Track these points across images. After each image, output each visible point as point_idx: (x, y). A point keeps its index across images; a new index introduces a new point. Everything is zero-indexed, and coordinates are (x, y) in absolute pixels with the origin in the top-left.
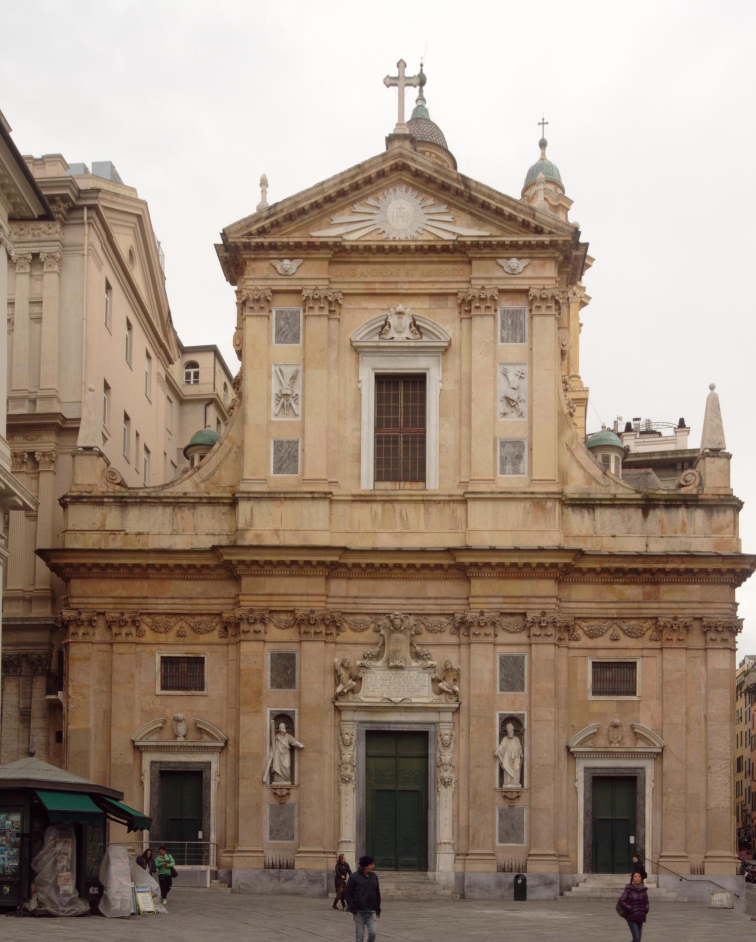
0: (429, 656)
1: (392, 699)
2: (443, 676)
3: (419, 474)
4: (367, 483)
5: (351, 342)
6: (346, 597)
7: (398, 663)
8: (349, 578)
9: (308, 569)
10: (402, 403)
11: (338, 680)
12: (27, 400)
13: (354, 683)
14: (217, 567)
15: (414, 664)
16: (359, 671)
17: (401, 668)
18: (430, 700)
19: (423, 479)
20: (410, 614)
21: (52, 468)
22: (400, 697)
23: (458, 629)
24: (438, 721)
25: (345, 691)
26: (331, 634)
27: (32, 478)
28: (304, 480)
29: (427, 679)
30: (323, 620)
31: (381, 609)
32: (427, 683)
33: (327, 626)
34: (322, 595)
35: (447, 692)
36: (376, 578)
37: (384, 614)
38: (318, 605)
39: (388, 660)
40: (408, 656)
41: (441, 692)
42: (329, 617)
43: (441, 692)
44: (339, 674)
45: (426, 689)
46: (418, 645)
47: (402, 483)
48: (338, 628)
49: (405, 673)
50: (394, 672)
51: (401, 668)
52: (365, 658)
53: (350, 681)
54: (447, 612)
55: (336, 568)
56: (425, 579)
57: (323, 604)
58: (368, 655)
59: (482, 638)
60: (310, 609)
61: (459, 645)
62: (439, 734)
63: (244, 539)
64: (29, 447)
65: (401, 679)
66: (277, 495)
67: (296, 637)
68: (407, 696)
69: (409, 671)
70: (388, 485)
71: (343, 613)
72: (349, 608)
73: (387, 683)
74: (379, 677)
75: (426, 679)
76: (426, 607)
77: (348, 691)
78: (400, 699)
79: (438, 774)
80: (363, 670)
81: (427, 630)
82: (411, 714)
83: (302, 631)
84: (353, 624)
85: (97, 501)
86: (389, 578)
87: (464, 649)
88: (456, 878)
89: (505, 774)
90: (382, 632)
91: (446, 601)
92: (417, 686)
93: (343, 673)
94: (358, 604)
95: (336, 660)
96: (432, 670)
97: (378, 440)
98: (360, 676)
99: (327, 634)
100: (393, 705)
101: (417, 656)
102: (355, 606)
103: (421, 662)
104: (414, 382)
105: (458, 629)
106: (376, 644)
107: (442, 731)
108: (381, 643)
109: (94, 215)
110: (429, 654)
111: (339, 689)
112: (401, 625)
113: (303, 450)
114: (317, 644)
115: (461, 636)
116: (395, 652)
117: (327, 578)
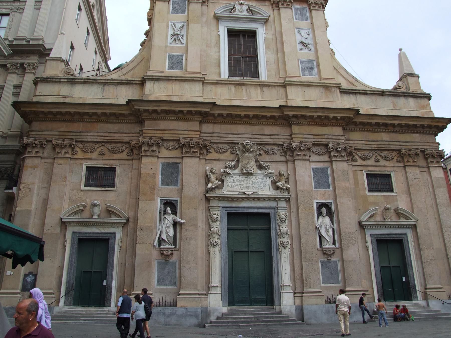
0: (269, 167)
1: (245, 192)
2: (278, 179)
4: (224, 74)
5: (215, 14)
6: (213, 133)
7: (249, 170)
8: (215, 123)
9: (189, 116)
11: (208, 180)
12: (25, 40)
13: (220, 182)
14: (130, 115)
15: (259, 172)
16: (222, 176)
17: (251, 174)
18: (271, 194)
19: (256, 75)
21: (34, 71)
22: (250, 191)
23: (285, 152)
24: (276, 206)
25: (214, 187)
26: (203, 153)
27: (20, 77)
28: (186, 72)
29: (268, 181)
30: (198, 145)
31: (235, 140)
32: (268, 183)
33: (201, 148)
34: (198, 131)
35: (282, 189)
36: (232, 124)
38: (195, 136)
39: (242, 170)
40: (255, 167)
41: (278, 188)
42: (202, 143)
43: (278, 188)
44: (209, 177)
45: (268, 187)
46: (261, 161)
48: (208, 151)
49: (254, 177)
50: (246, 176)
51: (251, 174)
52: (226, 168)
53: (217, 181)
54: (278, 143)
55: (207, 116)
56: (263, 125)
57: (198, 136)
58: (229, 166)
59: (301, 158)
61: (287, 162)
62: (277, 214)
64: (21, 61)
65: (251, 181)
66: (170, 78)
67: (181, 156)
68: (255, 191)
69: (256, 176)
71: (211, 143)
72: (215, 139)
74: (236, 179)
75: (268, 181)
76: (264, 140)
77: (215, 187)
79: (278, 240)
80: (224, 175)
81: (265, 153)
82: (258, 202)
83: (184, 151)
84: (217, 148)
86: (240, 124)
87: (290, 165)
88: (297, 309)
89: (322, 239)
90: (237, 153)
91: (277, 137)
92: (262, 185)
93: (213, 177)
94: (220, 137)
95: (207, 168)
96: (270, 176)
98: (223, 178)
99: (200, 154)
100: (247, 196)
101: (260, 167)
102: (219, 138)
103: (263, 171)
104: (249, 36)
105: (285, 152)
106: (233, 161)
107: (280, 212)
108: (236, 159)
110: (269, 165)
111: (210, 185)
112: (250, 148)
113: (186, 59)
114: (193, 159)
115: (288, 157)
116: (246, 164)
117: (201, 122)
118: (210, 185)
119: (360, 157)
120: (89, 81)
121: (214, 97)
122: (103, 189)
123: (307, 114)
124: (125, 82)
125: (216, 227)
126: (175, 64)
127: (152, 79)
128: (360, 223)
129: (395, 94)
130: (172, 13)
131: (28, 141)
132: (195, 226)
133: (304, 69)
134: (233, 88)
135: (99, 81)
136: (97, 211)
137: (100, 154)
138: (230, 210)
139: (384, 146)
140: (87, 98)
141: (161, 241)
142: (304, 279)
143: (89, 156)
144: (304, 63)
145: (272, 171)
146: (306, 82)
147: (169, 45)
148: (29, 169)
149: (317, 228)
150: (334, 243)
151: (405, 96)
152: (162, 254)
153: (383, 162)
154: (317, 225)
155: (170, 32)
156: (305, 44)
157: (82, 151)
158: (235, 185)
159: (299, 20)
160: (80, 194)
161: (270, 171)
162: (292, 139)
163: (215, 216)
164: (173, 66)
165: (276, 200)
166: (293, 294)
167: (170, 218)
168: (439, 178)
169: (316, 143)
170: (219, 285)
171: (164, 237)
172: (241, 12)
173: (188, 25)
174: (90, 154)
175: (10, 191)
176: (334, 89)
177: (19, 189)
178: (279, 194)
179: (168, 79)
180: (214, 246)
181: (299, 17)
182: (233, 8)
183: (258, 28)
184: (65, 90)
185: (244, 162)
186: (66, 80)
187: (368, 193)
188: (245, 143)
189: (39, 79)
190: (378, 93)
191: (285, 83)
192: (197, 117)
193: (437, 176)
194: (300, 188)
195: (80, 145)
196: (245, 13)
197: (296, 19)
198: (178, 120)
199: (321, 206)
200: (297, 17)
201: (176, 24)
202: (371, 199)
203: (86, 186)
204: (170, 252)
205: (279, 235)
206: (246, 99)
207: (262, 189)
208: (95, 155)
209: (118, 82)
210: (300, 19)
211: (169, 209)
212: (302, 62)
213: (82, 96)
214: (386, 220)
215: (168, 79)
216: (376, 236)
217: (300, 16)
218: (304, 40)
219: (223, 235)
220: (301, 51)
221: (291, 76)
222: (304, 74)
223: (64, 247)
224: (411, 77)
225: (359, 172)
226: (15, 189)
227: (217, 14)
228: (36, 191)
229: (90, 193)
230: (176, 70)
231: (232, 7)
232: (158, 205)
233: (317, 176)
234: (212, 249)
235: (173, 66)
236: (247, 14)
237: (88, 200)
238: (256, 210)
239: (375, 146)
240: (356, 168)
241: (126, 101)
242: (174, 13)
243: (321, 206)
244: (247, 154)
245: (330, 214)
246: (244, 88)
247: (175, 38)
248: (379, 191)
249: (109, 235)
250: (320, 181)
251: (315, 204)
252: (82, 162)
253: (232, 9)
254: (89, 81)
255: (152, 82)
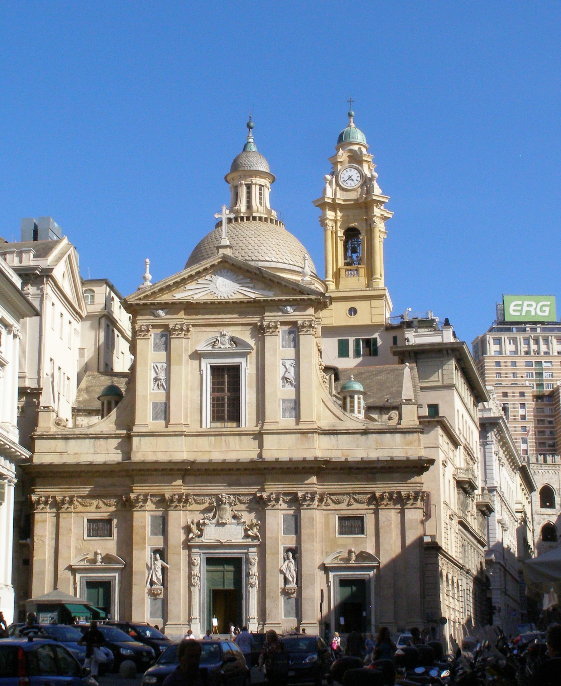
3: (235, 416)
10: (226, 380)
13: (199, 533)
15: (234, 521)
17: (226, 524)
20: (231, 494)
22: (224, 539)
37: (216, 494)
40: (230, 518)
46: (235, 510)
47: (226, 423)
60: (173, 493)
63: (136, 457)
65: (226, 530)
70: (218, 424)
73: (218, 532)
76: (240, 490)
78: (225, 540)
85: (53, 437)
86: (219, 475)
93: (194, 527)
97: (213, 399)
101: (235, 517)
109: (50, 280)
118: (191, 535)
119: (333, 502)
120: (81, 436)
121: (195, 450)
122: (103, 538)
123: (278, 466)
124: (113, 435)
125: (196, 570)
126: (159, 413)
127: (138, 436)
128: (324, 565)
129: (380, 431)
130: (154, 351)
131: (35, 498)
132: (179, 569)
133: (284, 410)
134: (213, 438)
135: (91, 436)
136: (99, 558)
137: (97, 507)
138: (208, 556)
139: (359, 489)
140: (81, 454)
141: (152, 583)
142: (267, 613)
143: (88, 509)
144: (286, 402)
145: (244, 520)
146: (282, 430)
147: (152, 391)
148: (39, 524)
149: (281, 572)
150: (297, 583)
151: (391, 433)
152: (154, 593)
153: (356, 506)
154: (282, 569)
155: (153, 375)
156: (289, 379)
157: (81, 504)
158: (213, 533)
159: (286, 347)
160: (84, 543)
161: (242, 520)
162: (265, 488)
163: (195, 561)
164: (157, 416)
165: (248, 546)
166: (257, 625)
167: (159, 563)
168: (412, 519)
169: (287, 492)
170: (198, 617)
171: (155, 579)
172: (223, 344)
173: (170, 366)
174: (89, 507)
175: (24, 541)
176: (310, 435)
177: (33, 541)
178: (249, 541)
179: (152, 434)
180: (194, 586)
181: (286, 343)
182: (216, 341)
183: (241, 363)
184: (59, 445)
185: (221, 513)
186: (60, 436)
187: (337, 535)
188: (220, 497)
189: (36, 437)
190: (360, 431)
191: (262, 431)
192: (179, 472)
193: (411, 518)
194: (268, 535)
195: (79, 500)
196: (228, 345)
197: (283, 347)
198: (163, 475)
199: (288, 550)
200: (284, 344)
201: (158, 365)
202: (340, 542)
203: (88, 536)
204: (159, 592)
205: (248, 577)
206: (224, 449)
207: (235, 537)
208: (93, 509)
209: (108, 436)
210: (287, 347)
211: (158, 556)
212: (284, 401)
213: (77, 452)
214: (351, 562)
215: (152, 434)
216: (339, 576)
217: (287, 343)
218: (287, 376)
219: (202, 578)
220: (283, 388)
221: (269, 422)
222: (284, 417)
223: (75, 589)
224: (406, 406)
225: (331, 516)
226: (28, 540)
227: (199, 351)
228: (47, 543)
229: (92, 542)
230: (160, 420)
231: (215, 340)
232: (148, 553)
233: (286, 522)
234: (193, 589)
235: (157, 416)
236: (230, 346)
237: (91, 548)
238: (230, 554)
239: (350, 489)
240: (329, 512)
241: (117, 448)
242: (156, 351)
243: (288, 550)
244: (223, 506)
245: (294, 558)
246: (223, 437)
247: (158, 384)
248: (351, 533)
249: (111, 578)
250: (289, 528)
251: (282, 549)
252: (83, 514)
253: (215, 342)
254: (81, 436)
255: (138, 438)
